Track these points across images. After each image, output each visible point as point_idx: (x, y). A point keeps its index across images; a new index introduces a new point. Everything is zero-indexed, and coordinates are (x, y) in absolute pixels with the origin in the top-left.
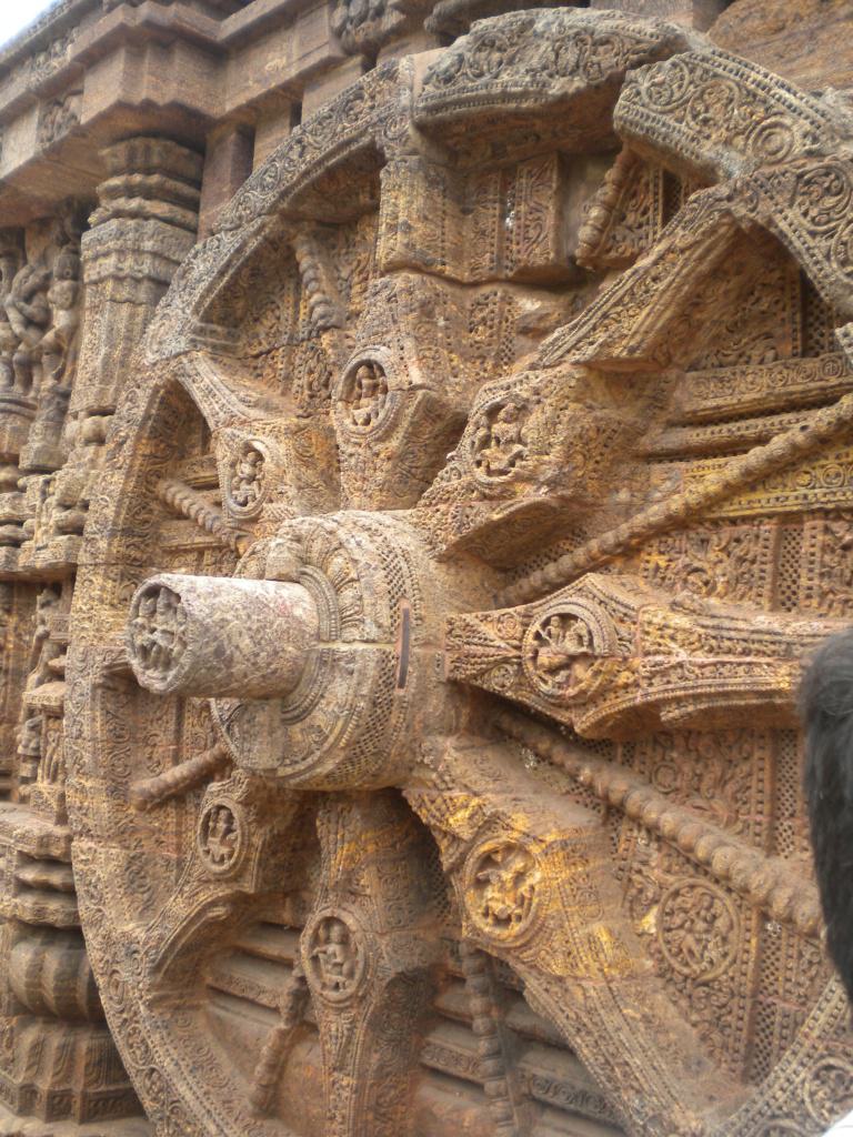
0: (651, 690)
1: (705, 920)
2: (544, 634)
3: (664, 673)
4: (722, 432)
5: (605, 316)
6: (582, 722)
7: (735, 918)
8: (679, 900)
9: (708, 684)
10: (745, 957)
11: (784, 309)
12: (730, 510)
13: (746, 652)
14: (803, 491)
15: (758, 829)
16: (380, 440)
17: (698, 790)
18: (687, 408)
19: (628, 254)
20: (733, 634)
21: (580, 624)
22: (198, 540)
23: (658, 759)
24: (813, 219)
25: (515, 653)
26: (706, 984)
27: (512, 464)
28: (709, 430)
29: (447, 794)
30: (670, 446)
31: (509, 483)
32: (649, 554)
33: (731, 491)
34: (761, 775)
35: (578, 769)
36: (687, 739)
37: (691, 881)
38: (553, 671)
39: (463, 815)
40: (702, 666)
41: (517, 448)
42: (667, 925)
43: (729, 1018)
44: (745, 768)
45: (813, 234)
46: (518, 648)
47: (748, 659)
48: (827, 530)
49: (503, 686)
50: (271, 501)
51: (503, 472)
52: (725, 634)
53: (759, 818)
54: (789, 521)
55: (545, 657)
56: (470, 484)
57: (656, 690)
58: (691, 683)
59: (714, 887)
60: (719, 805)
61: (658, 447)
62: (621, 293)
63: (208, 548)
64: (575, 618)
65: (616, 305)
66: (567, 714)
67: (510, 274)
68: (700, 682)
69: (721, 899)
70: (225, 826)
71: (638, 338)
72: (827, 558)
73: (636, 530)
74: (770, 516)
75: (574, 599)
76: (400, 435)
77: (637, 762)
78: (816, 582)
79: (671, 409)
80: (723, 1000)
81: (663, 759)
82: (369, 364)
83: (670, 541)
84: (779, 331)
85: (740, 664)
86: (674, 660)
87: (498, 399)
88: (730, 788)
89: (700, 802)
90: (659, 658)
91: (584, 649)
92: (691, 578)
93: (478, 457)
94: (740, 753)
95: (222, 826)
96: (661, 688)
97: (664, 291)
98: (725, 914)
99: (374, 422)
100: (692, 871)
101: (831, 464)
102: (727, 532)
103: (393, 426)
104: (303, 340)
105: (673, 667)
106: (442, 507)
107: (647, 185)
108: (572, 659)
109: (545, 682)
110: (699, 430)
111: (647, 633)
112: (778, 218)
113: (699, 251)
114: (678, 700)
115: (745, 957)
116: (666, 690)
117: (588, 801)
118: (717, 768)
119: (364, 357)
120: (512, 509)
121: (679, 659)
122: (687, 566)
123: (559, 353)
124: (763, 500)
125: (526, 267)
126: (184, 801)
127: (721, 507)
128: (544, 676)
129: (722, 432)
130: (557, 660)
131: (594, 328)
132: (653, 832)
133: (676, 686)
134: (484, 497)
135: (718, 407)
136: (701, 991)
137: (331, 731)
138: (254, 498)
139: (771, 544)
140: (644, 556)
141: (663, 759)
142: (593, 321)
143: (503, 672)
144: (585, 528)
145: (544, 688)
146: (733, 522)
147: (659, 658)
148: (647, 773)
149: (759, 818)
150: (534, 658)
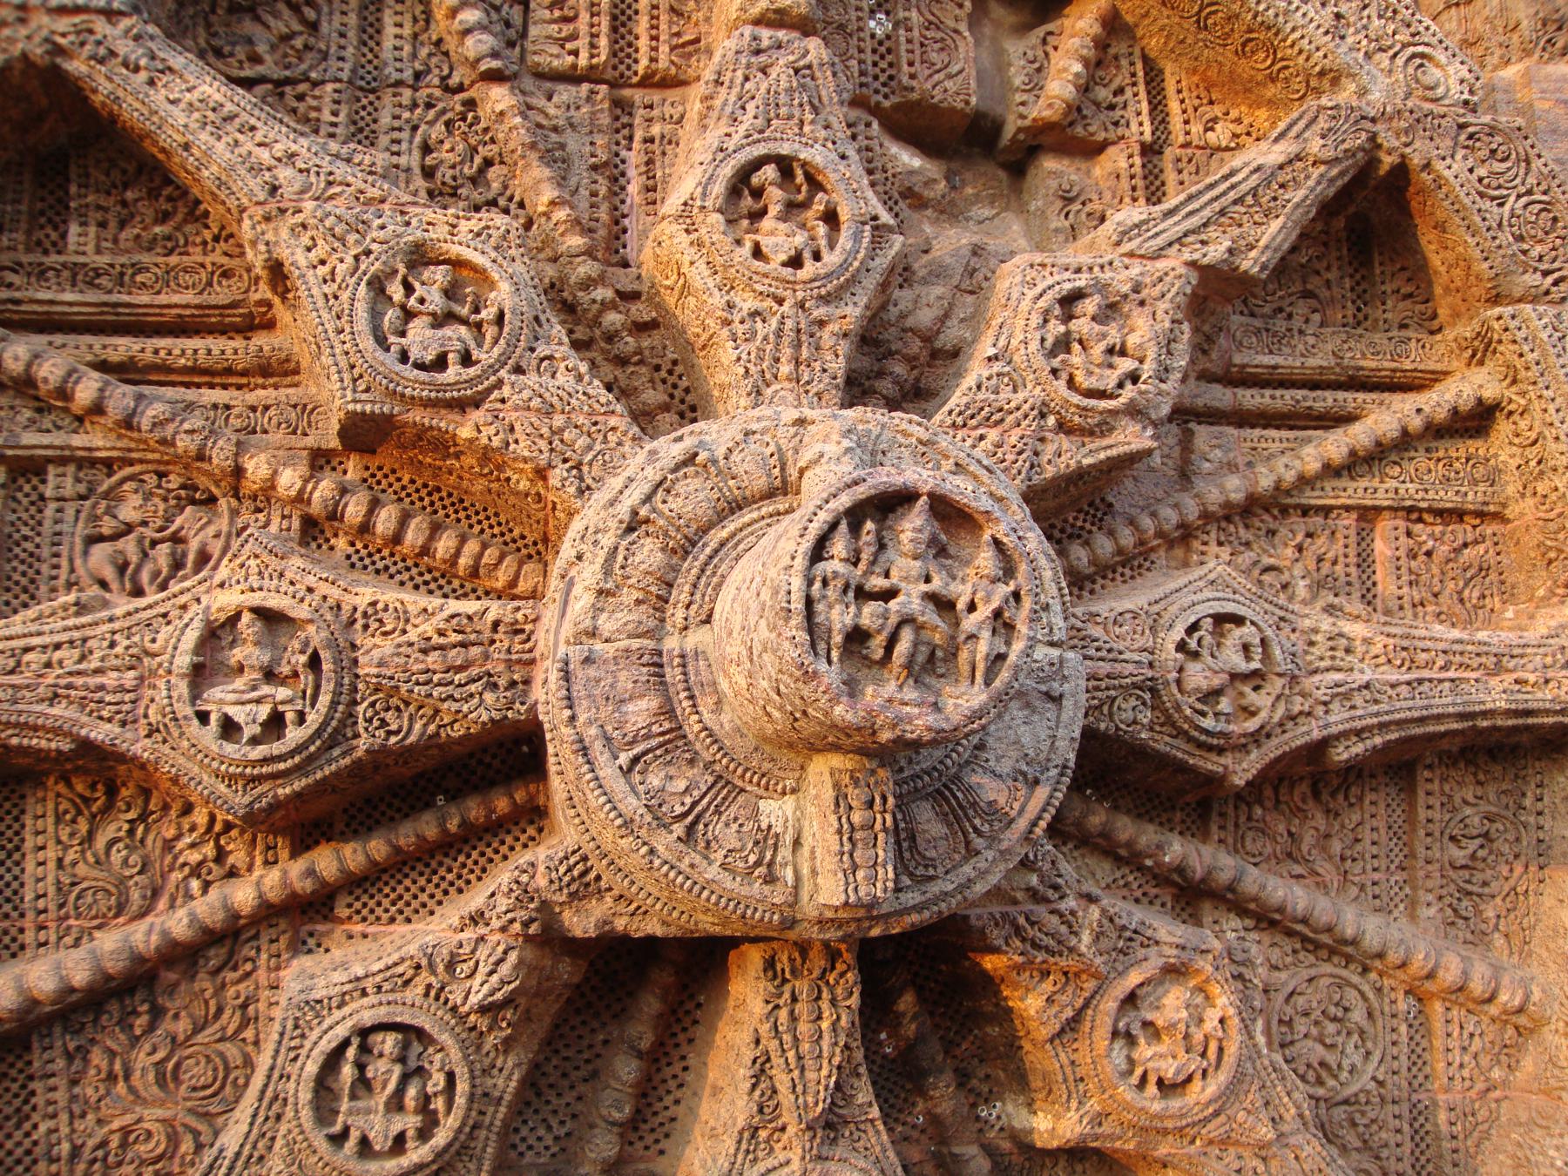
0: (1332, 718)
1: (1335, 1019)
2: (1193, 644)
3: (1347, 696)
4: (1285, 399)
5: (1222, 213)
6: (1242, 770)
7: (1376, 1005)
8: (1300, 1001)
9: (1405, 706)
10: (1395, 1051)
11: (1328, 268)
12: (1311, 498)
13: (1444, 668)
14: (1394, 483)
15: (1377, 890)
16: (825, 300)
17: (1289, 855)
18: (1238, 359)
19: (1101, 136)
20: (1429, 644)
21: (1247, 629)
22: (29, 438)
23: (1242, 819)
24: (1480, 180)
25: (1150, 674)
26: (1346, 1102)
27: (1120, 385)
28: (1268, 392)
29: (1063, 906)
30: (1217, 404)
31: (1114, 413)
32: (1205, 543)
33: (1331, 471)
34: (1375, 823)
35: (1159, 847)
36: (1276, 790)
37: (1313, 972)
38: (1214, 694)
39: (1086, 937)
40: (1393, 686)
41: (1126, 365)
42: (1289, 1038)
43: (1384, 1135)
44: (1356, 817)
45: (1482, 195)
46: (1151, 665)
47: (1451, 674)
48: (1409, 534)
49: (1135, 722)
50: (518, 370)
51: (1102, 394)
52: (1421, 644)
53: (1376, 876)
54: (1368, 515)
55: (1199, 676)
56: (1044, 404)
57: (1338, 718)
58: (1384, 707)
59: (1344, 973)
60: (1326, 869)
61: (1200, 402)
62: (1244, 188)
63: (62, 461)
64: (1238, 620)
65: (1235, 202)
66: (1222, 760)
67: (887, 104)
68: (1398, 705)
69: (1356, 987)
70: (397, 1070)
71: (1268, 254)
72: (1413, 564)
73: (1212, 508)
74: (1348, 508)
75: (1208, 594)
76: (863, 300)
77: (1214, 828)
78: (1406, 590)
79: (1214, 356)
80: (1372, 1115)
81: (1249, 819)
82: (785, 165)
83: (1232, 528)
84: (1324, 293)
85: (1441, 681)
86: (1360, 678)
87: (1078, 284)
88: (1336, 847)
89: (1298, 869)
90: (1338, 676)
91: (1255, 665)
92: (1266, 578)
93: (1056, 362)
94: (1346, 798)
95: (386, 1072)
96: (1347, 715)
97: (1297, 206)
98: (1361, 1003)
99: (809, 269)
100: (1312, 958)
101: (1421, 460)
102: (1300, 525)
103: (853, 281)
104: (399, 83)
105: (1359, 689)
106: (993, 435)
107: (1116, 58)
108: (1235, 677)
109: (1203, 714)
110: (1254, 391)
111: (1312, 644)
112: (1439, 166)
113: (1335, 172)
114: (1358, 733)
115: (1395, 1051)
116: (1352, 719)
117: (1138, 894)
118: (1320, 821)
119: (785, 149)
120: (1114, 452)
121: (1366, 678)
122: (1255, 563)
123: (1160, 241)
124: (1356, 491)
125: (919, 103)
126: (28, 1048)
127: (1301, 491)
128: (1199, 706)
129: (1285, 399)
130: (1217, 681)
131: (1205, 225)
132: (1268, 919)
133: (1365, 712)
134: (1063, 427)
135: (1275, 367)
136: (1340, 1113)
137: (1021, 812)
138: (466, 360)
139: (1353, 539)
140: (1196, 544)
141: (1249, 819)
142: (1207, 213)
143: (1133, 702)
144: (1110, 499)
145: (1208, 723)
146: (1305, 511)
147: (1338, 676)
148: (1230, 841)
149: (1376, 876)
150: (1179, 682)
